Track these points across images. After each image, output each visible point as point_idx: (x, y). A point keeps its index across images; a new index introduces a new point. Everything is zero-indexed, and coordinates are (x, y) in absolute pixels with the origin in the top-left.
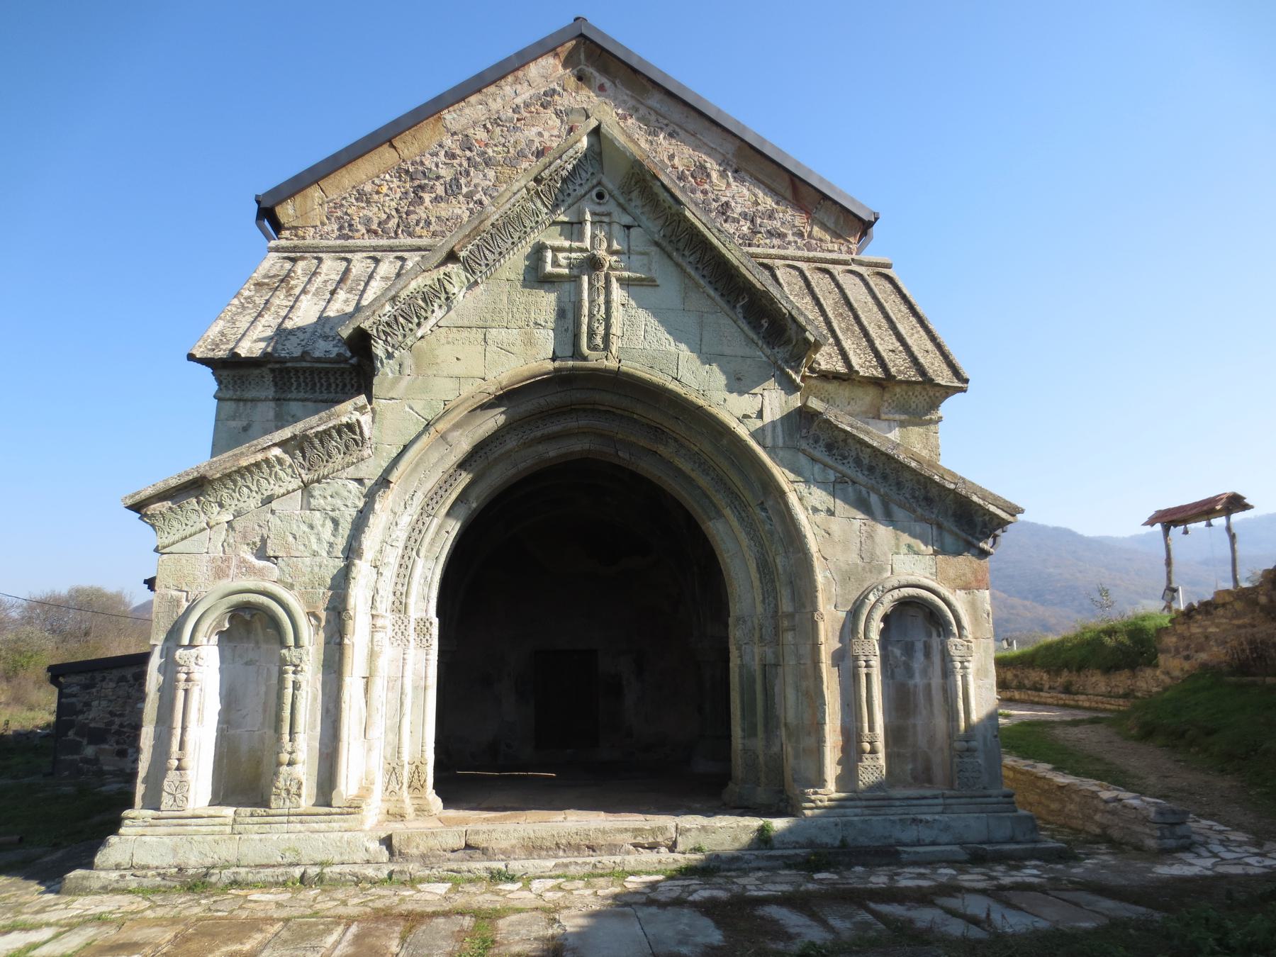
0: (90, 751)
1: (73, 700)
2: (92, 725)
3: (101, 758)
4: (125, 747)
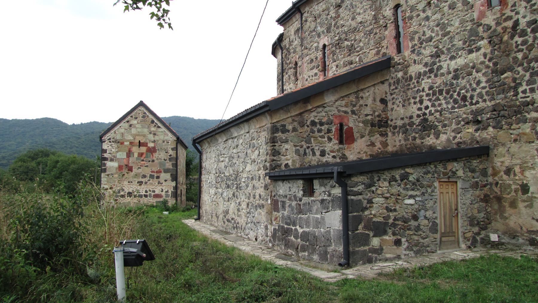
0: (375, 242)
1: (360, 197)
2: (374, 220)
3: (384, 247)
4: (399, 237)
